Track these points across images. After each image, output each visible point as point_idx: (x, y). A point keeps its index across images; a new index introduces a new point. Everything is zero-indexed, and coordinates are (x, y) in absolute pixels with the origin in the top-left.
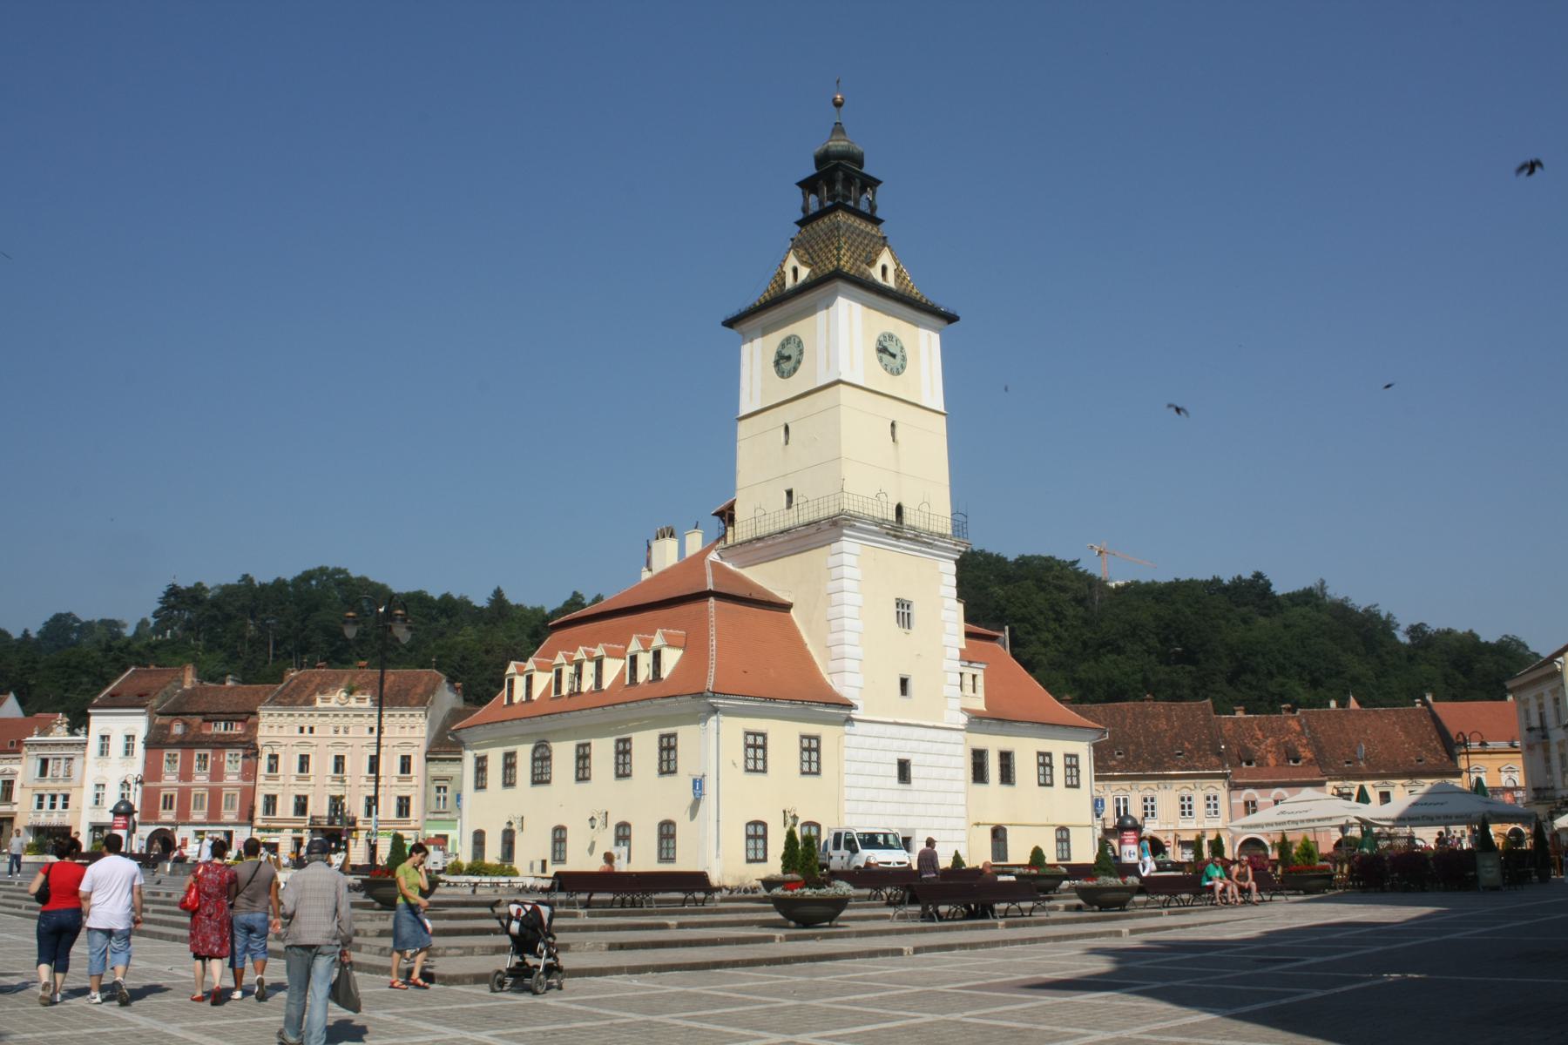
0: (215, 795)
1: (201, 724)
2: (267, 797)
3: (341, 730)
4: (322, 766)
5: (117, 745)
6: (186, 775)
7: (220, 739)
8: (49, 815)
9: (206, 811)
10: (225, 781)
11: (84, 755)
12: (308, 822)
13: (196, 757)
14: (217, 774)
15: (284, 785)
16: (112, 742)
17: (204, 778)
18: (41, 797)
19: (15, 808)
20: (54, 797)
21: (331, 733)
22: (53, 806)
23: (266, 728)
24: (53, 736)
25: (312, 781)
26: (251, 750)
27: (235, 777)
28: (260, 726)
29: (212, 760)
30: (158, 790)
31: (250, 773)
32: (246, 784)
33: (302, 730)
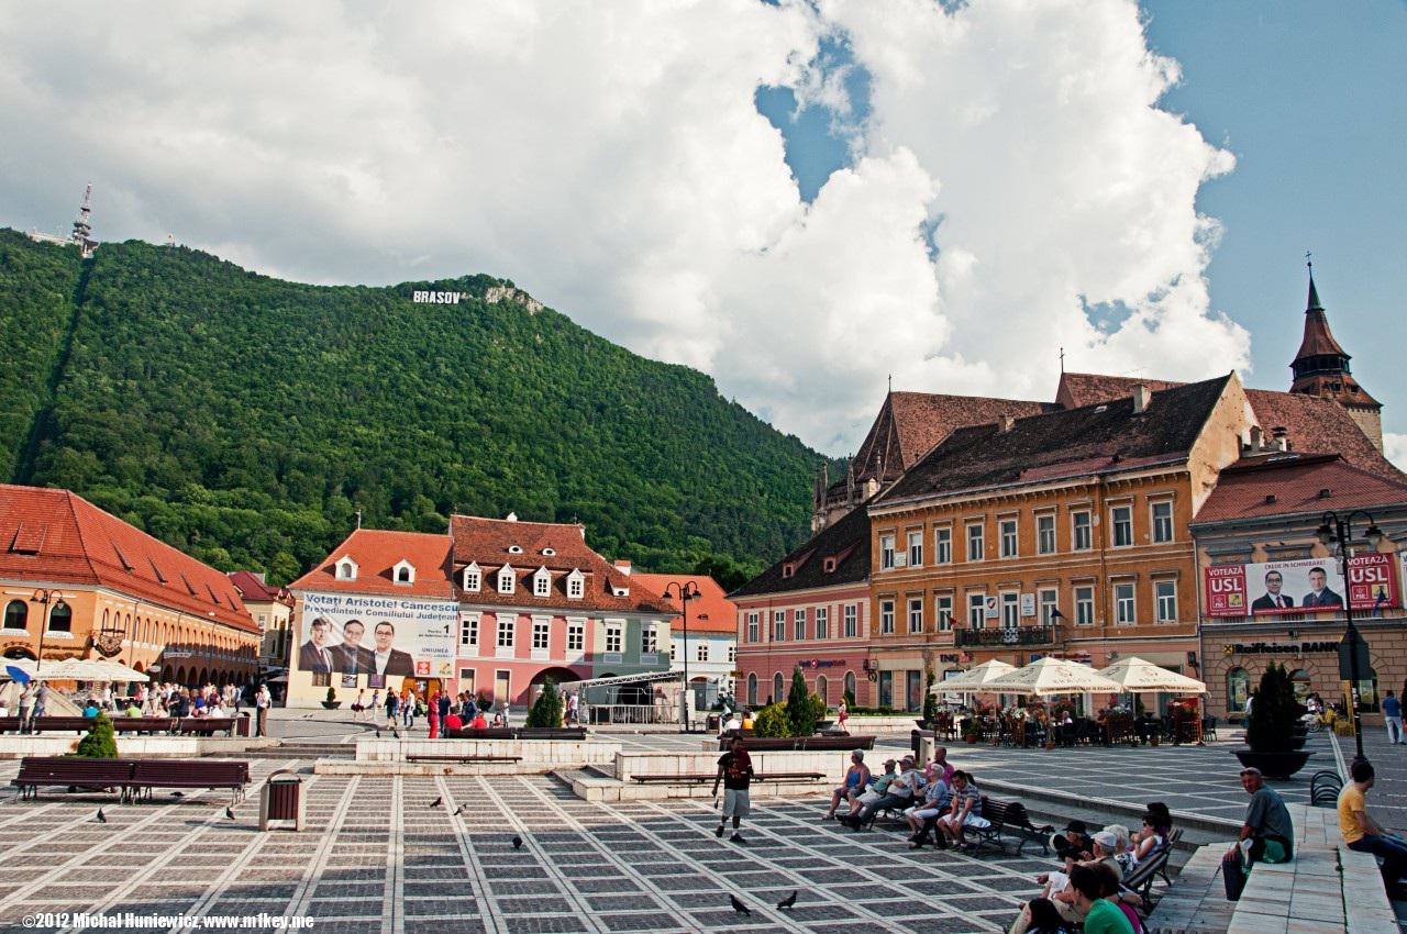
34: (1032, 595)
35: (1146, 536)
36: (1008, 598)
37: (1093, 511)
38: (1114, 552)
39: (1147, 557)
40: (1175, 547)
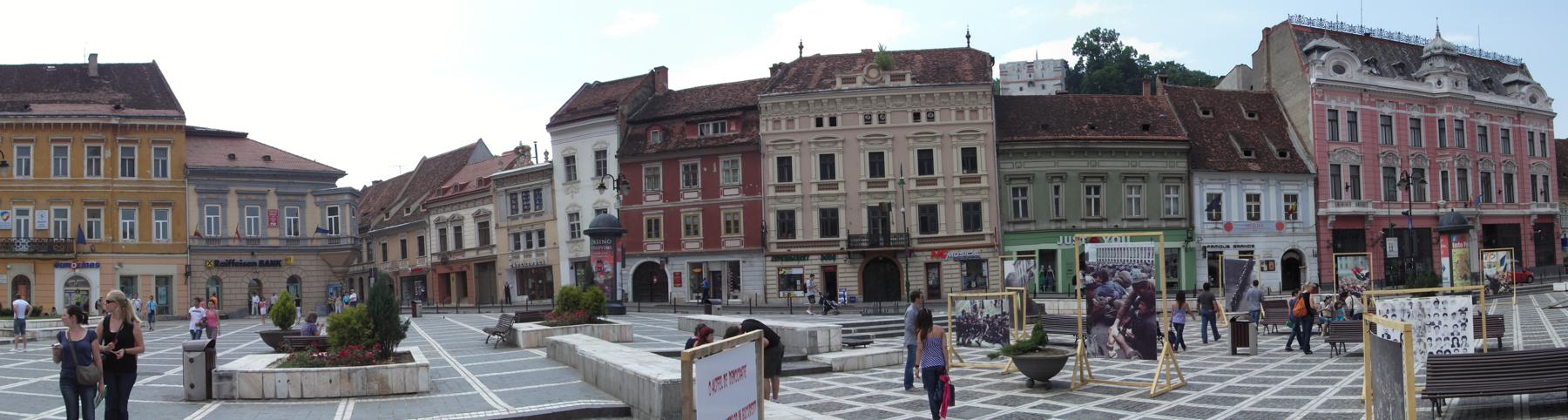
0: (711, 215)
1: (683, 129)
2: (781, 214)
3: (875, 118)
4: (852, 169)
5: (586, 167)
6: (671, 193)
7: (710, 143)
8: (539, 253)
9: (701, 236)
10: (722, 197)
11: (552, 182)
12: (843, 245)
13: (681, 170)
14: (711, 188)
15: (802, 197)
16: (579, 164)
17: (695, 195)
18: (517, 236)
19: (495, 252)
20: (529, 235)
21: (861, 124)
22: (530, 245)
23: (770, 123)
24: (518, 167)
25: (841, 189)
26: (752, 153)
27: (736, 191)
28: (762, 121)
29: (702, 170)
30: (639, 214)
31: (752, 183)
32: (751, 198)
33: (819, 122)
34: (47, 212)
35: (149, 172)
36: (20, 212)
37: (105, 146)
38: (120, 182)
39: (147, 188)
40: (171, 182)
